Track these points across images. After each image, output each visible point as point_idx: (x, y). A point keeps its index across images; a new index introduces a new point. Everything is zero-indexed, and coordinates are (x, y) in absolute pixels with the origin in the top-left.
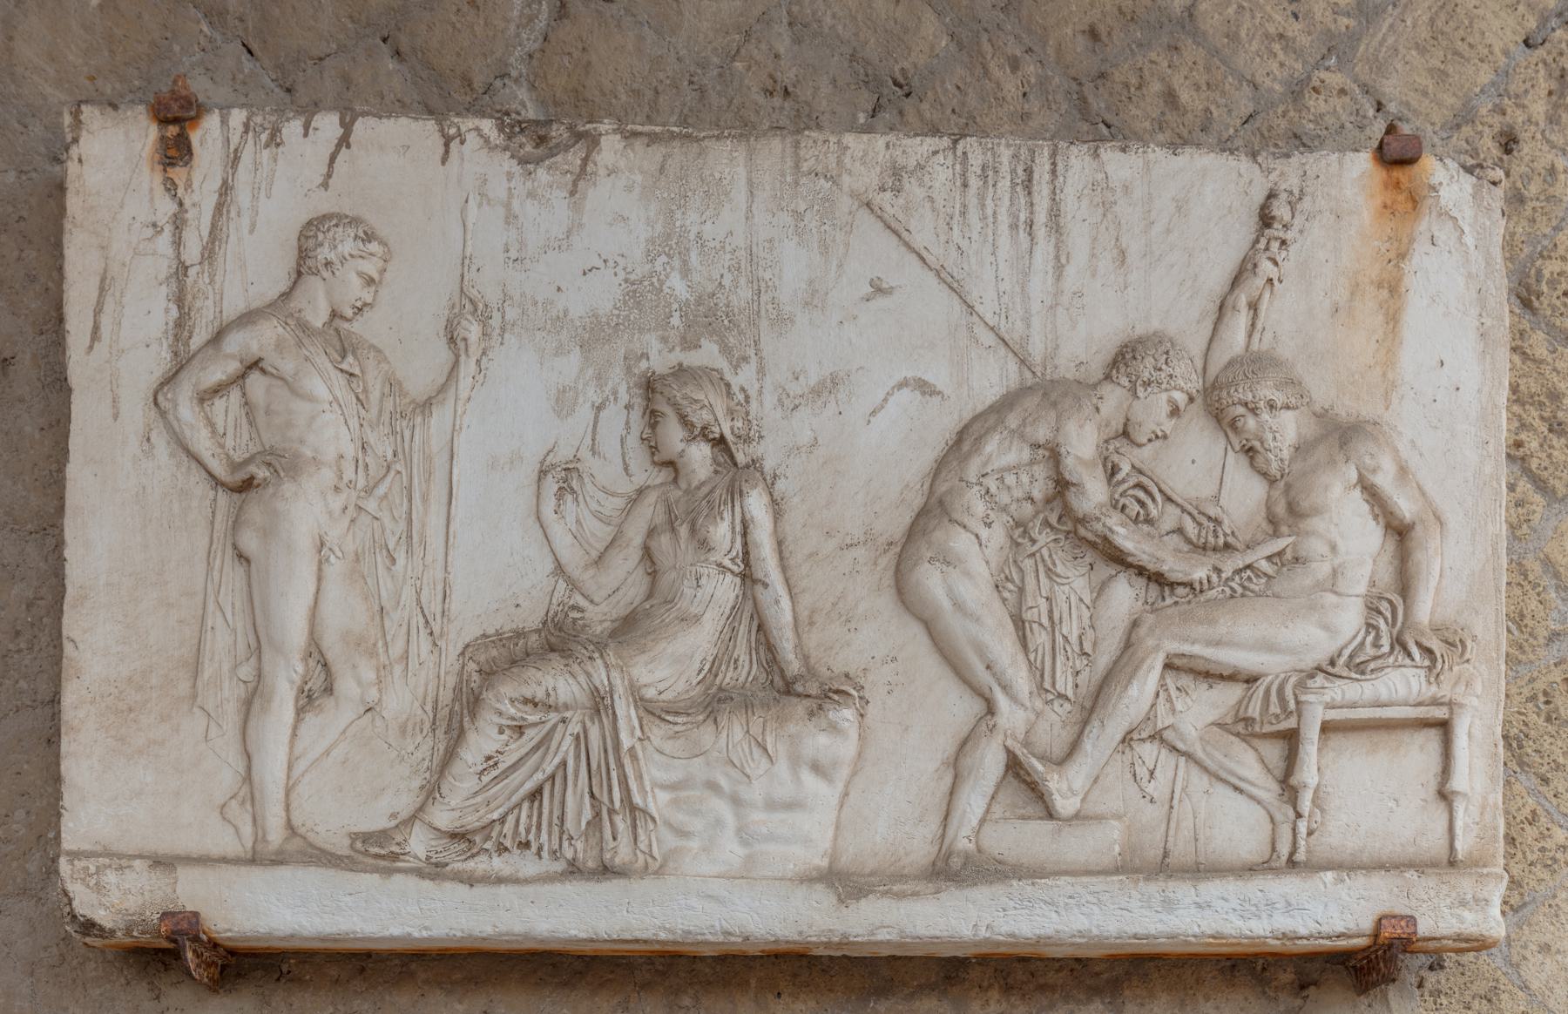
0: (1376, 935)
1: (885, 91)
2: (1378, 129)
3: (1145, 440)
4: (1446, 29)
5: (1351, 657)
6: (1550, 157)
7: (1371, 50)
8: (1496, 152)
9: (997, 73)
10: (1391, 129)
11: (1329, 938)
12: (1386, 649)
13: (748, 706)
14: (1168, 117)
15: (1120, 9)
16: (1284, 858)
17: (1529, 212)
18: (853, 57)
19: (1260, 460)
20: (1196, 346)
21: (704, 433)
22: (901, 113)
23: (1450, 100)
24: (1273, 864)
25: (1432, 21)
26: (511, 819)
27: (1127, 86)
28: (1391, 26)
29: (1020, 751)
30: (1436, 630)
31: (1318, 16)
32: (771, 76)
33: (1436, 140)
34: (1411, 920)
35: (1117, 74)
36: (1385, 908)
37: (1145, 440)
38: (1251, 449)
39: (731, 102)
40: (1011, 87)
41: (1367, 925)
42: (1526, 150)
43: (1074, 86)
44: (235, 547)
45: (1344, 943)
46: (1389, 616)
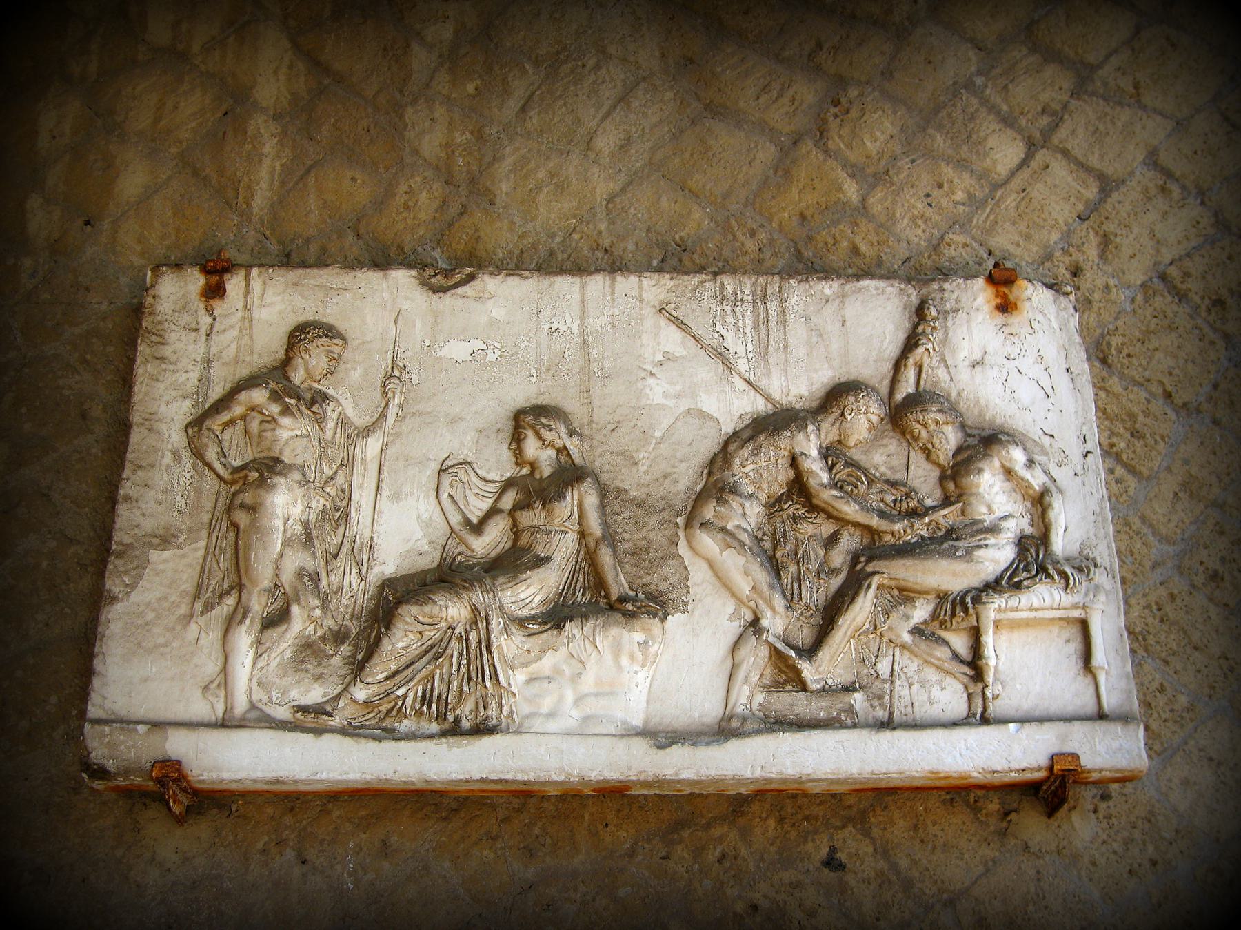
0: (1051, 769)
1: (670, 248)
2: (990, 264)
3: (852, 444)
4: (1026, 211)
5: (1010, 578)
6: (1105, 279)
7: (981, 222)
8: (1068, 276)
9: (742, 238)
10: (996, 265)
11: (1017, 771)
12: (1034, 572)
13: (585, 617)
14: (854, 260)
15: (818, 203)
16: (978, 716)
17: (1096, 309)
18: (648, 230)
19: (933, 457)
20: (884, 389)
21: (551, 445)
22: (680, 261)
23: (1035, 249)
24: (970, 720)
25: (1017, 207)
26: (411, 696)
27: (826, 244)
28: (992, 210)
29: (780, 646)
30: (1067, 560)
31: (944, 204)
32: (595, 241)
33: (1029, 270)
34: (1075, 757)
35: (818, 237)
36: (1056, 750)
37: (852, 444)
38: (926, 448)
39: (570, 256)
40: (751, 245)
41: (1043, 761)
42: (1088, 275)
43: (791, 244)
44: (229, 519)
45: (1029, 775)
46: (1033, 551)
